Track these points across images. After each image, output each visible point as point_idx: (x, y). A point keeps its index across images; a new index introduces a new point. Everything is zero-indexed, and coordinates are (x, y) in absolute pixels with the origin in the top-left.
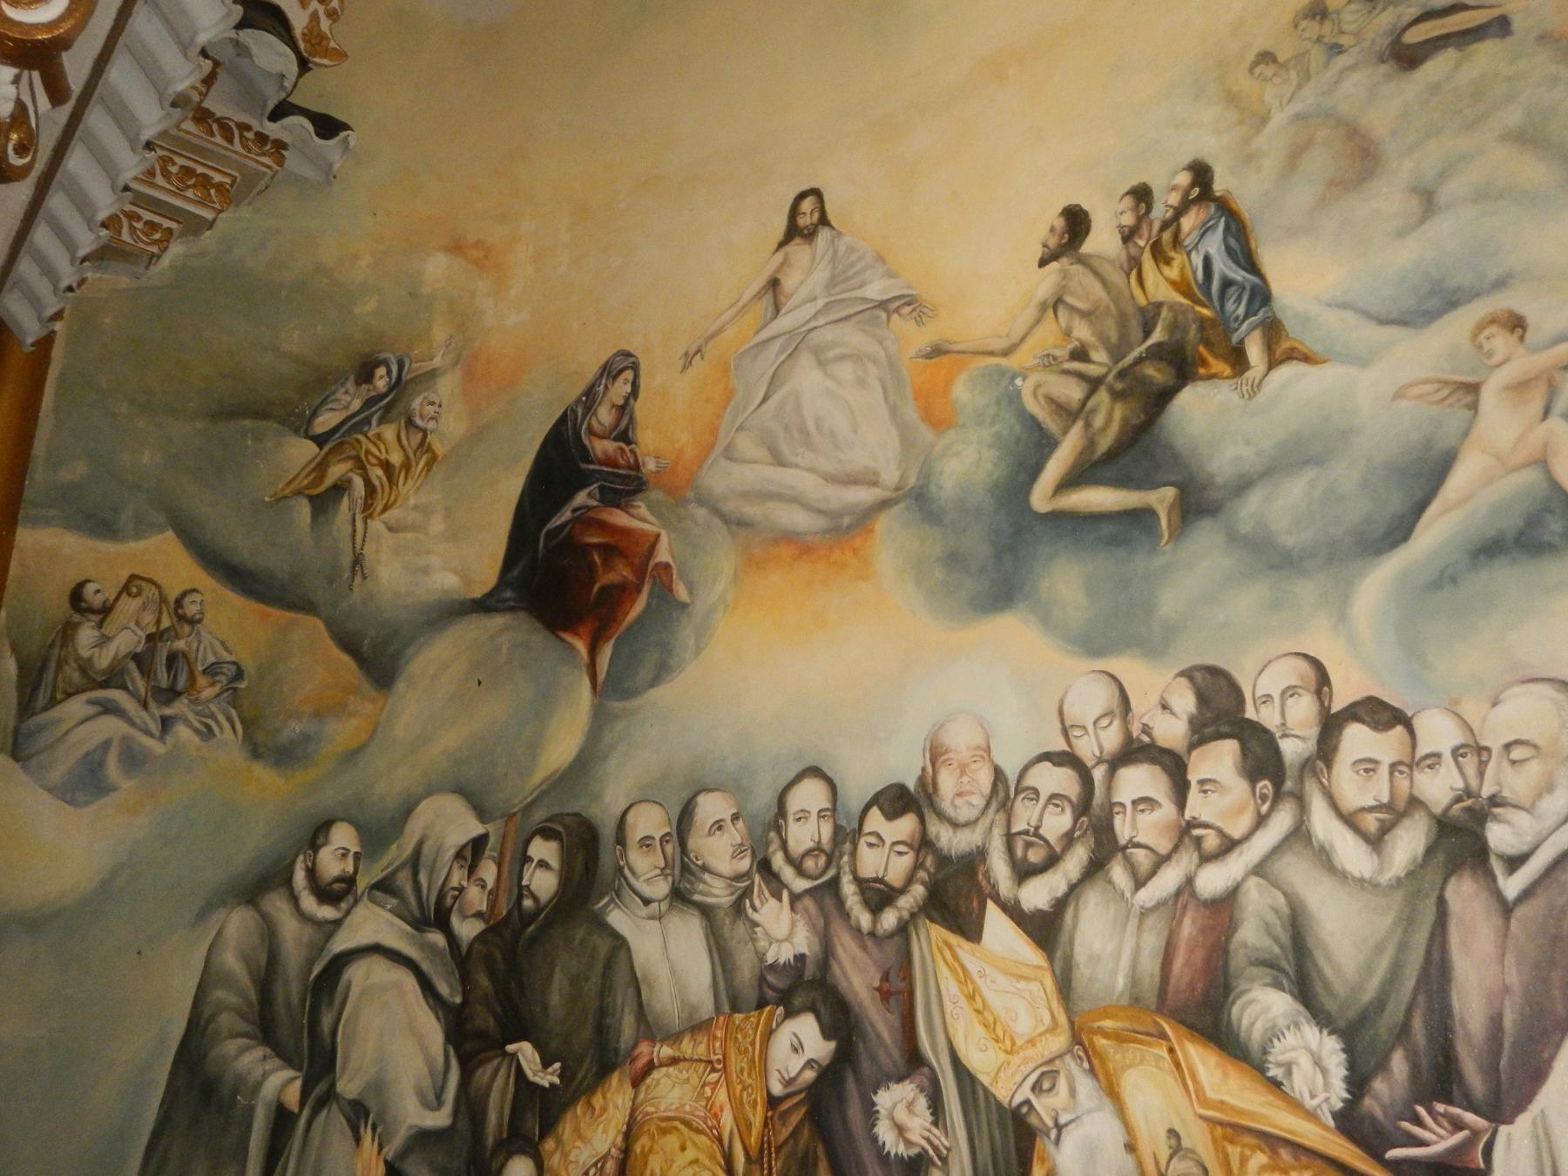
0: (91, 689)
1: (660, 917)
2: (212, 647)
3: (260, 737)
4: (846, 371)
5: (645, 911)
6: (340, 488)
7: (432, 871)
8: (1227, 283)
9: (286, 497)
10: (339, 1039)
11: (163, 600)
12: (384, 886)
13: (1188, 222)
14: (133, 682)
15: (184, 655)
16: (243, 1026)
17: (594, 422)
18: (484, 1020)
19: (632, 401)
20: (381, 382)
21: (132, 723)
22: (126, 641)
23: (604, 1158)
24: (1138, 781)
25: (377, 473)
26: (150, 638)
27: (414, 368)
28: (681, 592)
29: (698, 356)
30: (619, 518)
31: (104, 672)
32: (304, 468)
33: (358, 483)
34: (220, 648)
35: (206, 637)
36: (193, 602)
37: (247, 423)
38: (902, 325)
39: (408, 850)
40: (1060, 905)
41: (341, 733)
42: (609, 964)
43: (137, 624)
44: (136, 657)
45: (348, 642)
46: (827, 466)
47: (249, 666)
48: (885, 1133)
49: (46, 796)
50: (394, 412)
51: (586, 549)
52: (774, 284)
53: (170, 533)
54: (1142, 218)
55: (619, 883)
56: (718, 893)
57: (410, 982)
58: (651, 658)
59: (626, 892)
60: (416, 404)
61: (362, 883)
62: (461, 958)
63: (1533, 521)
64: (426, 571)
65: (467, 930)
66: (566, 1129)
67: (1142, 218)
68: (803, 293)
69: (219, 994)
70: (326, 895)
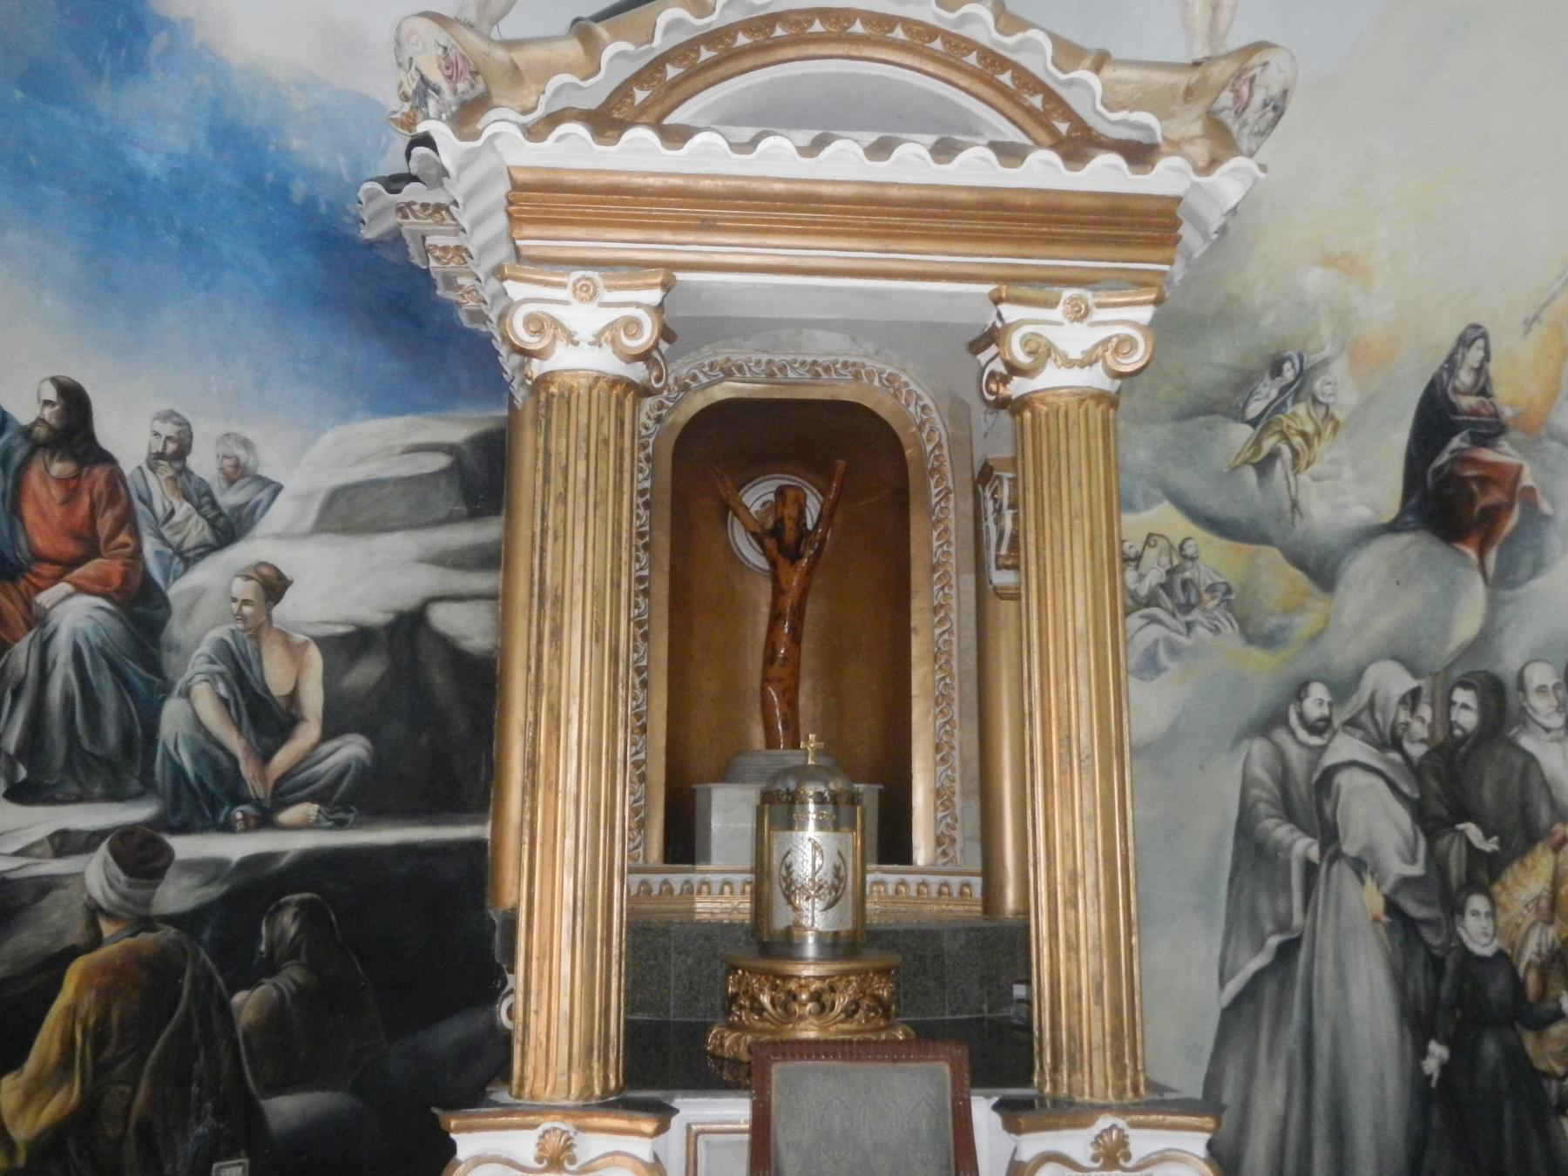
0: (1140, 609)
1: (1558, 740)
2: (1208, 574)
3: (1250, 630)
5: (1548, 736)
6: (1273, 455)
7: (1384, 712)
9: (1237, 467)
10: (1339, 818)
11: (1171, 547)
12: (1352, 723)
14: (1164, 602)
15: (1192, 581)
16: (1274, 811)
17: (1458, 384)
18: (1438, 808)
19: (1486, 365)
20: (1289, 373)
21: (1167, 627)
22: (1154, 575)
23: (1538, 898)
25: (1297, 441)
26: (1169, 572)
27: (1312, 359)
28: (1546, 507)
29: (1535, 324)
30: (1487, 455)
31: (1146, 597)
32: (1246, 444)
33: (1286, 450)
34: (1211, 573)
35: (1202, 568)
36: (1191, 546)
37: (1202, 419)
41: (1305, 623)
42: (1525, 773)
43: (1159, 564)
44: (1162, 586)
45: (1298, 561)
47: (1234, 584)
50: (1302, 395)
51: (1465, 481)
53: (1167, 503)
55: (1524, 718)
57: (1380, 784)
58: (1528, 558)
59: (1532, 725)
60: (1317, 385)
61: (1337, 722)
62: (1415, 770)
64: (1345, 506)
65: (1417, 751)
66: (1508, 877)
70: (1314, 728)
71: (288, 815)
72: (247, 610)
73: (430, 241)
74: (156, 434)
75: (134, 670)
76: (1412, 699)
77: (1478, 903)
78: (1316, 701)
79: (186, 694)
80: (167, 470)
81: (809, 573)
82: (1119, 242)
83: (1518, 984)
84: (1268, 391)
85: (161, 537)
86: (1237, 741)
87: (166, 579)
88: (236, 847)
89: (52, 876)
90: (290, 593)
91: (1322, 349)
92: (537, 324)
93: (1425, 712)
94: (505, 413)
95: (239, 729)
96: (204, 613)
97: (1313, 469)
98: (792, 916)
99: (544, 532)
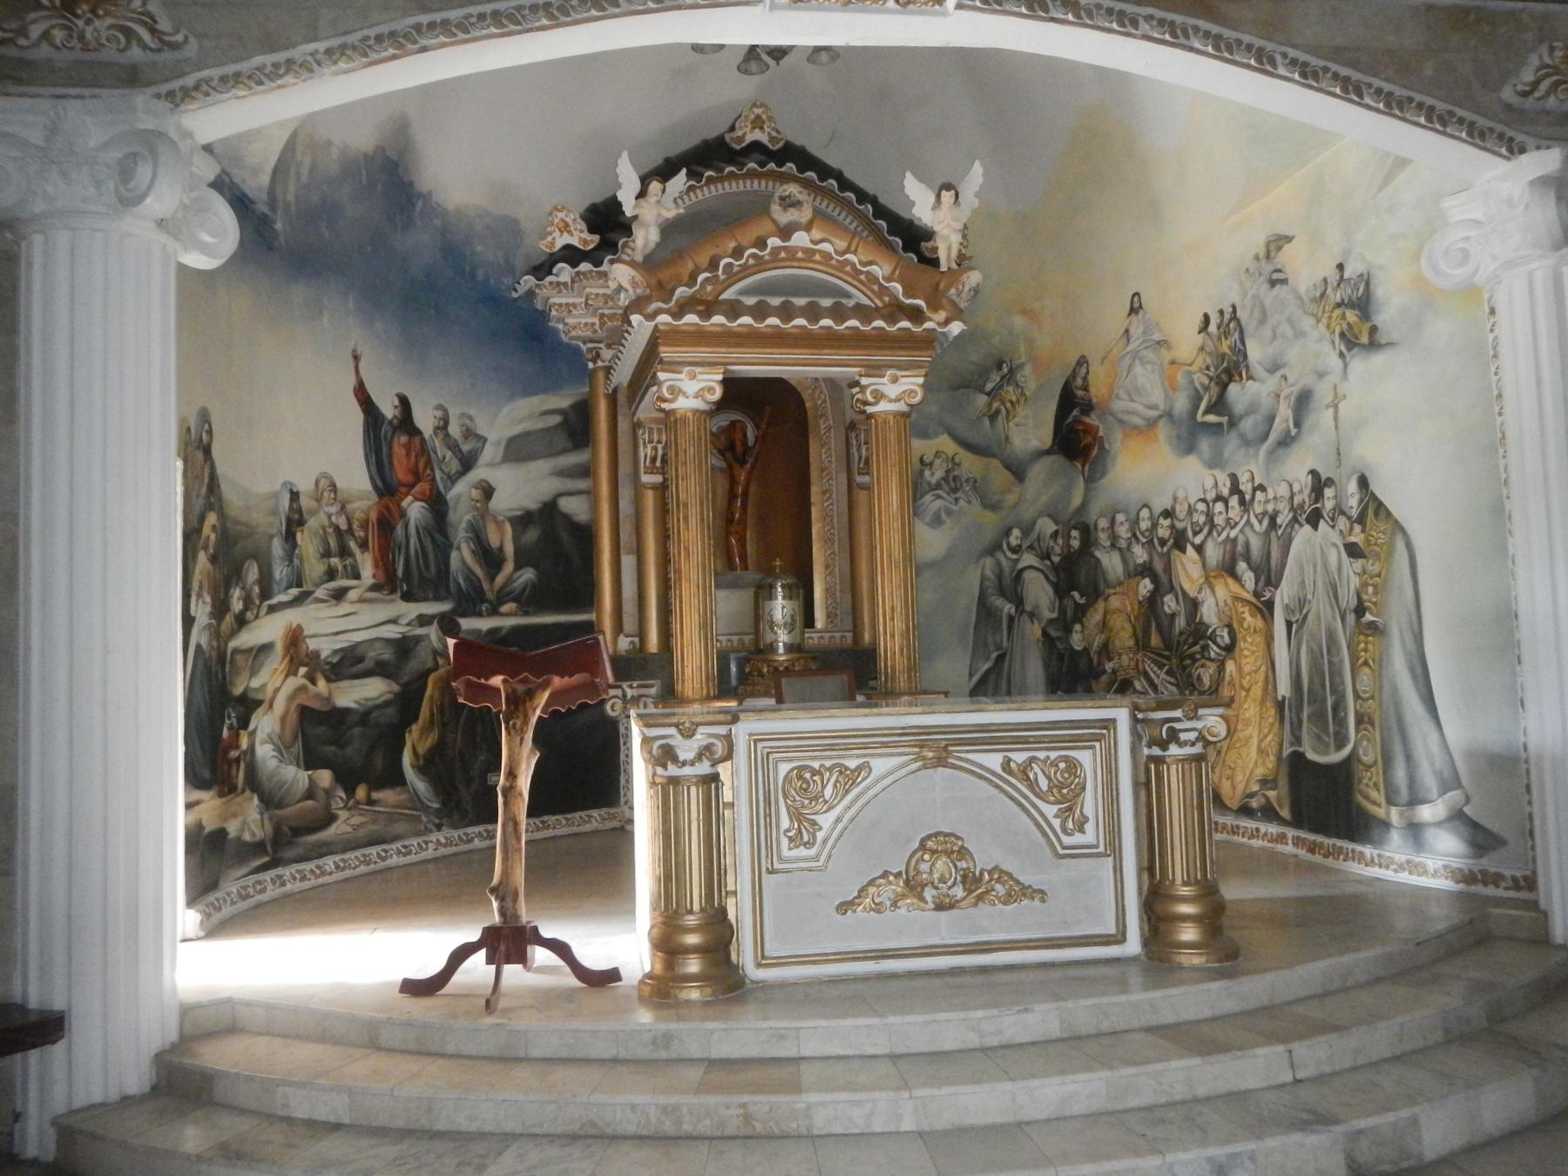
1: (1108, 552)
4: (1149, 367)
5: (1104, 550)
6: (998, 412)
8: (1239, 350)
11: (947, 457)
12: (1031, 547)
13: (1232, 325)
20: (1005, 370)
22: (939, 474)
24: (1219, 507)
25: (1008, 405)
26: (946, 471)
27: (1016, 362)
28: (1107, 446)
33: (1003, 409)
38: (1164, 351)
39: (1036, 536)
40: (1203, 543)
41: (1010, 499)
44: (943, 479)
45: (1008, 467)
46: (1145, 402)
48: (1166, 608)
49: (926, 527)
52: (1127, 331)
53: (946, 435)
54: (1222, 321)
55: (1096, 543)
56: (1123, 544)
57: (1042, 576)
60: (1018, 377)
61: (1024, 547)
62: (1055, 568)
63: (1286, 438)
64: (1029, 441)
65: (1056, 559)
66: (1088, 615)
67: (1222, 321)
68: (1135, 336)
69: (987, 583)
71: (505, 608)
72: (478, 505)
73: (552, 300)
74: (435, 417)
75: (438, 537)
76: (1055, 535)
77: (1078, 627)
78: (1015, 537)
79: (459, 548)
80: (441, 436)
81: (750, 472)
82: (910, 348)
83: (1091, 660)
84: (995, 378)
85: (441, 469)
86: (977, 561)
87: (445, 487)
88: (484, 624)
89: (421, 636)
90: (495, 496)
91: (1020, 358)
92: (672, 389)
93: (1060, 541)
94: (587, 389)
95: (480, 565)
96: (462, 507)
97: (1016, 420)
98: (774, 637)
99: (677, 477)
